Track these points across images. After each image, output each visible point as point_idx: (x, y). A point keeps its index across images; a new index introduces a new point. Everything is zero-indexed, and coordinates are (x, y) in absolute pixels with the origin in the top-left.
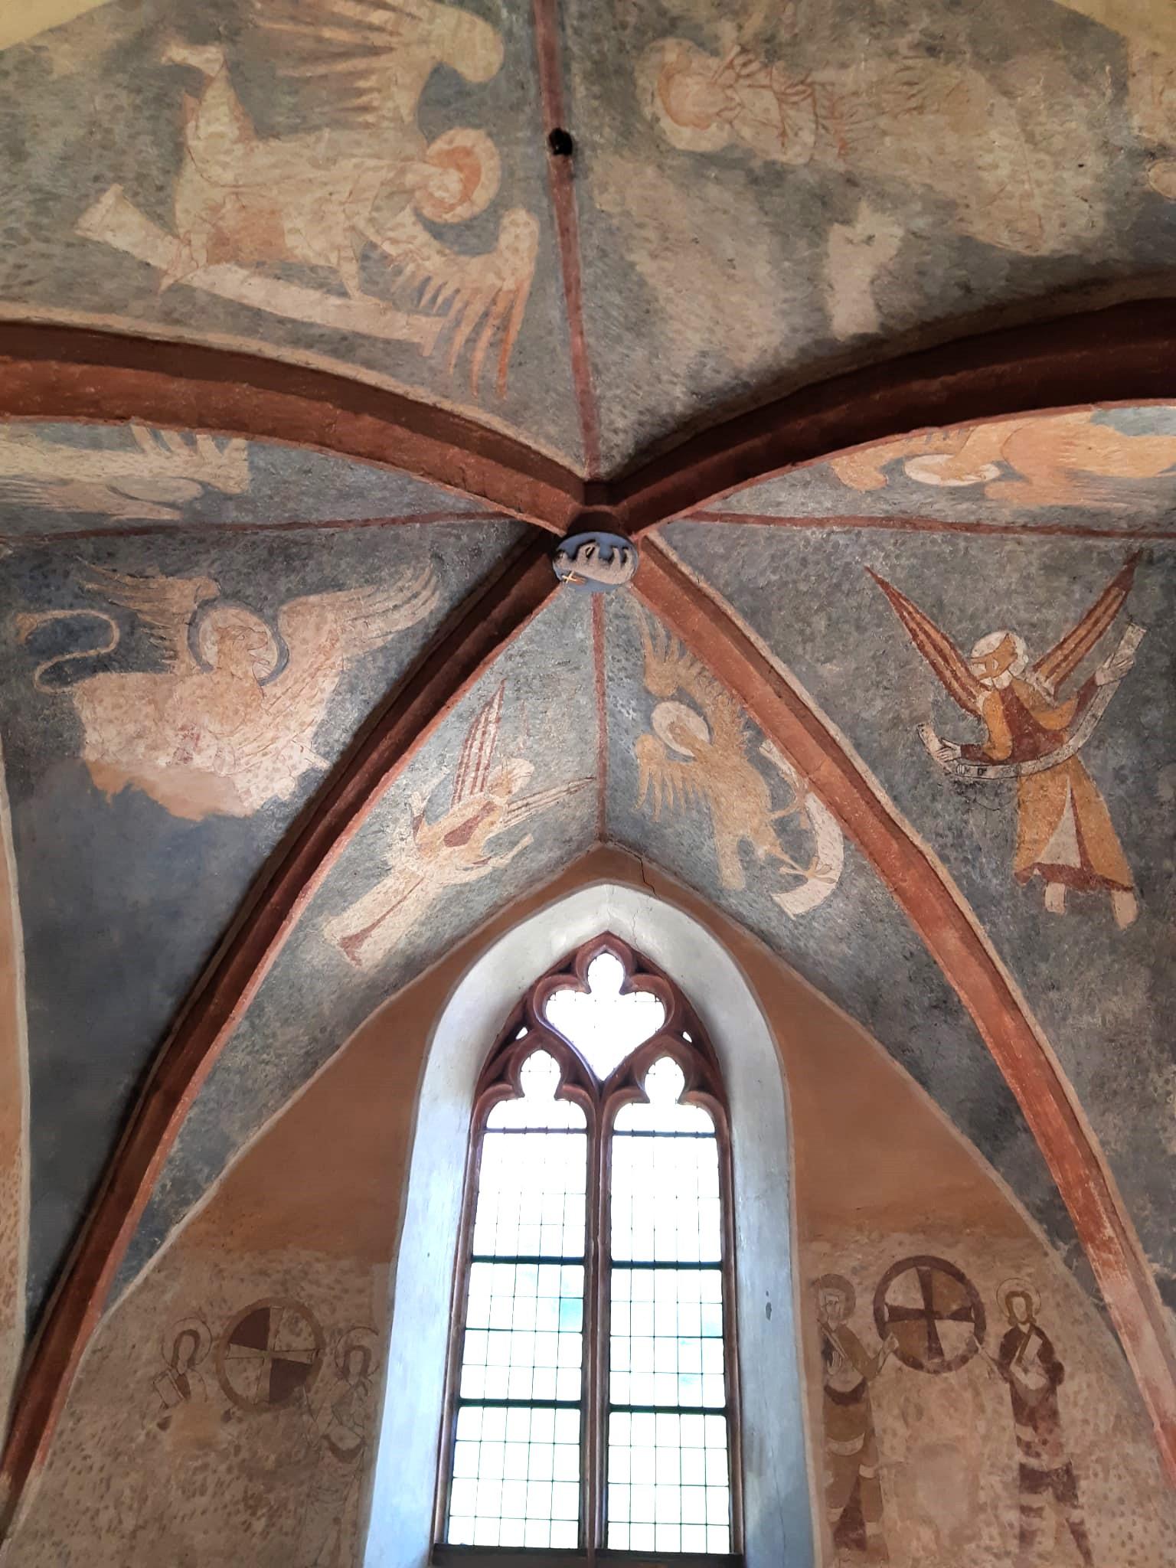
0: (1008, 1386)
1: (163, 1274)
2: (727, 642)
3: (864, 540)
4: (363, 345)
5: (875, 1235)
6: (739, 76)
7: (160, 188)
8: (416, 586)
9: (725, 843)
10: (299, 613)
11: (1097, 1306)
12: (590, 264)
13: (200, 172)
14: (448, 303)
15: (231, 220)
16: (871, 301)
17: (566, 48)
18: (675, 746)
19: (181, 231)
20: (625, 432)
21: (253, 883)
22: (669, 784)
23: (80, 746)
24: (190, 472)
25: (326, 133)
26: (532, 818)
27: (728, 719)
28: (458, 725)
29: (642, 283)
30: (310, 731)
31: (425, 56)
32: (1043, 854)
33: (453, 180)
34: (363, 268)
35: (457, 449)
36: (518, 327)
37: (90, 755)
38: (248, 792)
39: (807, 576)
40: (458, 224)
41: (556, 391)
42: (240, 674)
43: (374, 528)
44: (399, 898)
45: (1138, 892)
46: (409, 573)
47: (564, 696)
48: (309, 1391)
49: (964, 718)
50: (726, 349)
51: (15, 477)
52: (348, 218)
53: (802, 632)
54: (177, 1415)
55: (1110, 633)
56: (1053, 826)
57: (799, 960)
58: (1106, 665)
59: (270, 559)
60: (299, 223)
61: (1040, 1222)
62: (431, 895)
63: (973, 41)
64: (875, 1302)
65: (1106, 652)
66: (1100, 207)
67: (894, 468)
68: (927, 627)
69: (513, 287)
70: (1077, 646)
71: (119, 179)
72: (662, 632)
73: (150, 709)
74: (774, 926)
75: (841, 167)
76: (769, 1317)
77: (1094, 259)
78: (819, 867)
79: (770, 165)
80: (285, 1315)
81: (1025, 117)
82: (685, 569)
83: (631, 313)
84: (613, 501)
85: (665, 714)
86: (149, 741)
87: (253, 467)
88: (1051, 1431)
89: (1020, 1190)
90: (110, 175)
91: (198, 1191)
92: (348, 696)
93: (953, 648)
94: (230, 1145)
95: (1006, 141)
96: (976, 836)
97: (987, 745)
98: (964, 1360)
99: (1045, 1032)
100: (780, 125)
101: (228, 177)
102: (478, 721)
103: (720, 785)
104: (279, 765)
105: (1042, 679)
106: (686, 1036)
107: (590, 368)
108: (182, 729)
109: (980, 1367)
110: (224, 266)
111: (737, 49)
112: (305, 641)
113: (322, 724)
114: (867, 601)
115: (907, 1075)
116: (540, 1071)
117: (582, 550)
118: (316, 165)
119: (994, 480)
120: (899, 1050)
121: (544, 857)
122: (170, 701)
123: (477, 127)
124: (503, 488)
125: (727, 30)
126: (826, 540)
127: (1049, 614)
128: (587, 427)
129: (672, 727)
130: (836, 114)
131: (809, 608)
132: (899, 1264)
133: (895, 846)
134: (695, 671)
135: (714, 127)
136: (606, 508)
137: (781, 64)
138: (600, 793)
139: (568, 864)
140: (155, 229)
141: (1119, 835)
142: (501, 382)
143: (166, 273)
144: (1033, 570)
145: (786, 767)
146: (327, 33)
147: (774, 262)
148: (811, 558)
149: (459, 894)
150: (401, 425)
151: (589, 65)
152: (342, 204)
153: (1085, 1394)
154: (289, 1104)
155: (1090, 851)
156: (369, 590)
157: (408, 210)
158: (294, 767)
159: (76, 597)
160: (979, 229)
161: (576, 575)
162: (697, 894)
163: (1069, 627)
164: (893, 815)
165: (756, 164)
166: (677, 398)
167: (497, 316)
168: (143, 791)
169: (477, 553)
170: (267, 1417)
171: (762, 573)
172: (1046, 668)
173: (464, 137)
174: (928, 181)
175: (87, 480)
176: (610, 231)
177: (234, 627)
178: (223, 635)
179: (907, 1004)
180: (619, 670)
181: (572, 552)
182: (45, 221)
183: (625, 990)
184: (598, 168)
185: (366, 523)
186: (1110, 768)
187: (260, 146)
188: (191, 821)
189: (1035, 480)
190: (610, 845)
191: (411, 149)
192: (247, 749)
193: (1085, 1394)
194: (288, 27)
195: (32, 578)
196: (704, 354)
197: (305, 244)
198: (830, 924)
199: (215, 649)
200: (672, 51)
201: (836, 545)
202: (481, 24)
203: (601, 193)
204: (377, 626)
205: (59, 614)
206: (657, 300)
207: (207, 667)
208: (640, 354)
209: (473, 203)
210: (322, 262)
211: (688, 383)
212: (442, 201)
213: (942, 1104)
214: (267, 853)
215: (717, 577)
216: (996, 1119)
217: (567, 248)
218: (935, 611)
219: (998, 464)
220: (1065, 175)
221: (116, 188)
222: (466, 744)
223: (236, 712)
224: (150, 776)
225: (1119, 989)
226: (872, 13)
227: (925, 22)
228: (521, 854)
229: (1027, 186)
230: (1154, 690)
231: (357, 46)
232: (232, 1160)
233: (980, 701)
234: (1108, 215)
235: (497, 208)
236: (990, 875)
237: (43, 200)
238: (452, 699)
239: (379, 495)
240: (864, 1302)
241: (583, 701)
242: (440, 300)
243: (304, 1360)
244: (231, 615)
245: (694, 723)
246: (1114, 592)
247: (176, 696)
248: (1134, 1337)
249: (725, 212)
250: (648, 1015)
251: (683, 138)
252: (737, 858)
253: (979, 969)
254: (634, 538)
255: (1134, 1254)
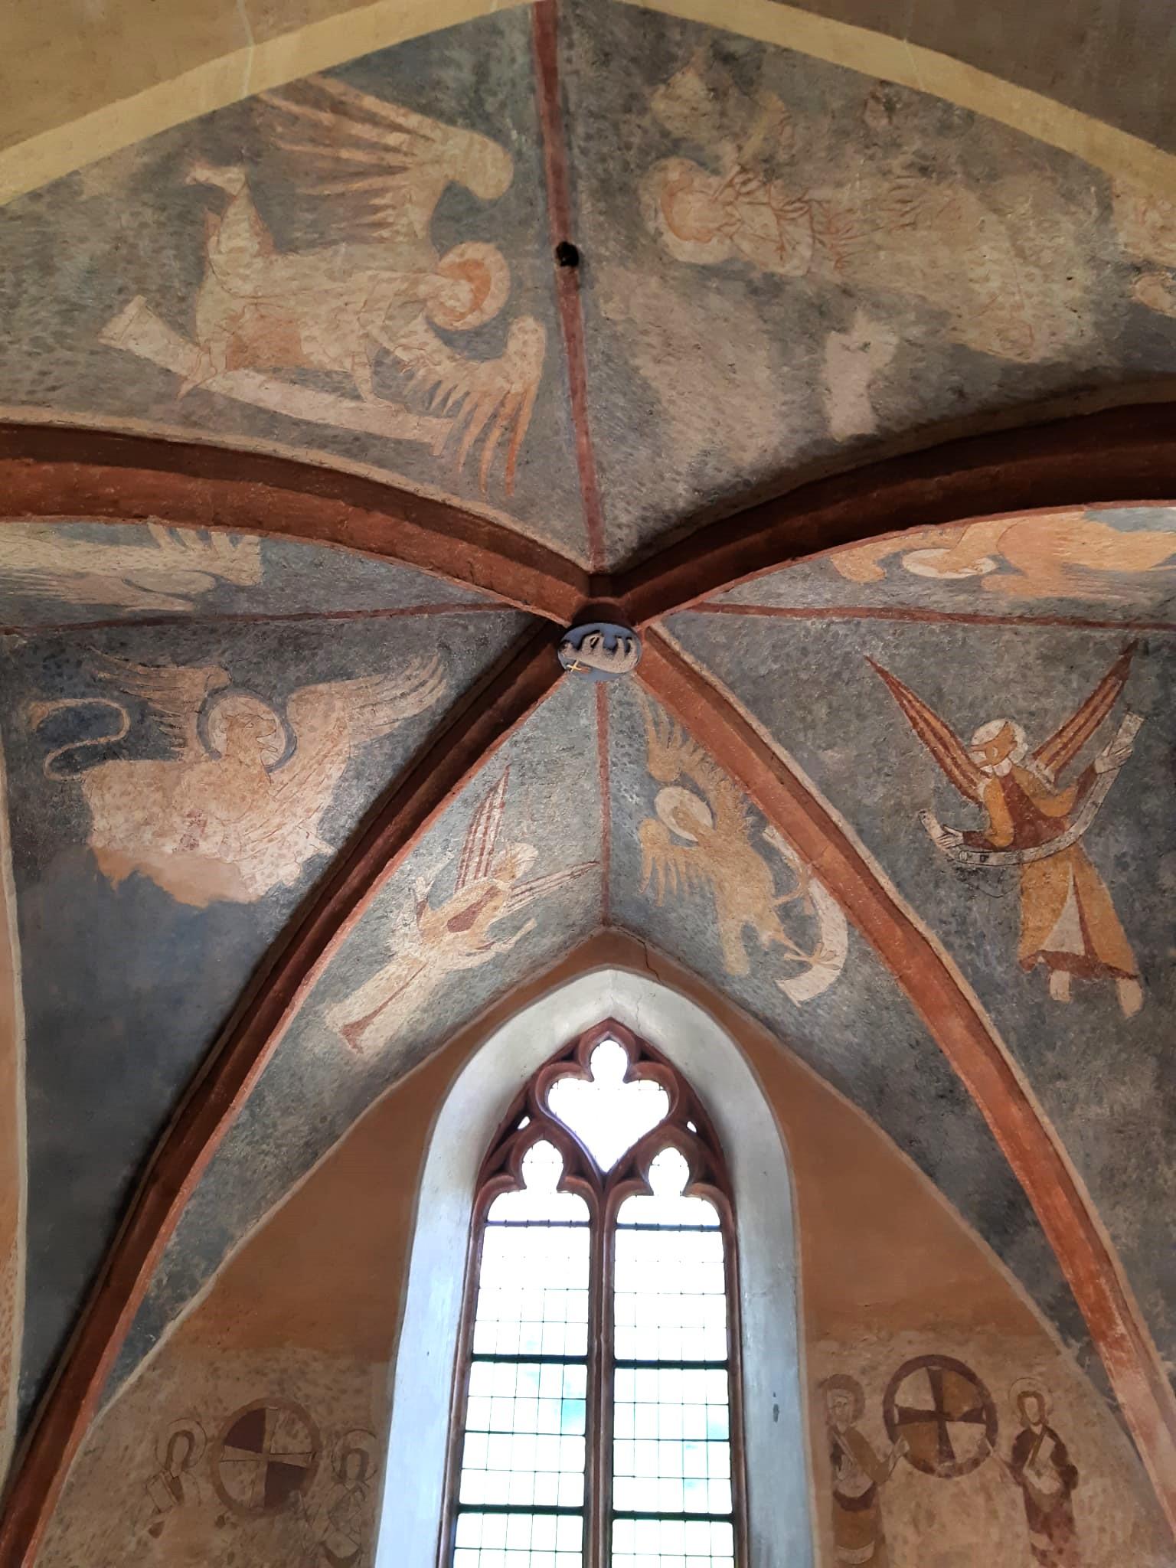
0: (1020, 1490)
1: (158, 1372)
2: (729, 728)
3: (863, 630)
4: (375, 446)
5: (883, 1334)
6: (739, 194)
7: (183, 299)
8: (424, 674)
9: (729, 929)
10: (307, 701)
11: (1110, 1406)
12: (595, 369)
13: (221, 284)
14: (458, 404)
15: (250, 327)
16: (868, 405)
17: (573, 168)
18: (678, 831)
19: (202, 339)
20: (629, 526)
21: (256, 970)
22: (673, 869)
23: (87, 833)
24: (204, 565)
25: (343, 248)
26: (535, 903)
27: (730, 804)
28: (462, 810)
29: (646, 386)
30: (316, 817)
31: (438, 175)
32: (1047, 942)
33: (464, 290)
34: (376, 373)
35: (465, 544)
36: (526, 428)
37: (97, 842)
38: (253, 878)
39: (808, 664)
40: (468, 331)
41: (561, 487)
42: (248, 761)
43: (383, 619)
44: (401, 984)
45: (1142, 979)
46: (417, 662)
47: (569, 781)
48: (305, 1495)
49: (965, 805)
50: (728, 449)
51: (32, 571)
52: (363, 326)
53: (804, 719)
54: (170, 1521)
55: (1108, 721)
56: (1056, 913)
57: (804, 1047)
58: (1105, 754)
59: (281, 649)
60: (316, 331)
61: (1052, 1318)
62: (434, 982)
63: (963, 162)
64: (885, 1402)
65: (1105, 741)
66: (1088, 317)
67: (892, 562)
68: (927, 715)
69: (521, 390)
70: (1075, 734)
71: (143, 291)
72: (664, 718)
73: (158, 796)
74: (778, 1013)
75: (837, 279)
76: (776, 1419)
77: (1084, 366)
78: (824, 953)
79: (769, 277)
80: (282, 1417)
81: (1015, 232)
82: (688, 658)
83: (635, 415)
84: (617, 594)
85: (668, 799)
86: (156, 828)
87: (265, 560)
88: (1066, 1540)
89: (1031, 1285)
90: (134, 287)
91: (195, 1287)
92: (355, 782)
93: (953, 735)
94: (227, 1238)
95: (996, 255)
96: (979, 924)
97: (990, 831)
98: (976, 1463)
99: (1053, 1122)
101: (248, 288)
102: (482, 806)
103: (724, 871)
104: (285, 851)
105: (1042, 766)
106: (691, 1126)
107: (595, 467)
108: (189, 816)
109: (991, 1471)
110: (243, 371)
111: (737, 168)
112: (313, 729)
113: (329, 809)
114: (868, 688)
115: (913, 1166)
116: (542, 1162)
117: (587, 640)
118: (331, 276)
119: (991, 573)
120: (907, 1142)
121: (548, 942)
122: (178, 790)
123: (488, 241)
124: (510, 580)
125: (727, 151)
126: (826, 631)
127: (1047, 702)
128: (592, 522)
129: (675, 812)
130: (833, 230)
131: (810, 696)
132: (909, 1362)
133: (899, 933)
134: (698, 756)
135: (715, 240)
136: (610, 600)
137: (779, 182)
138: (604, 879)
139: (572, 949)
140: (175, 337)
141: (1122, 922)
142: (508, 480)
143: (186, 379)
144: (1030, 659)
145: (789, 853)
146: (345, 154)
148: (811, 648)
149: (462, 980)
150: (412, 521)
151: (595, 183)
152: (358, 313)
153: (1101, 1499)
154: (287, 1196)
155: (1094, 938)
156: (377, 678)
157: (420, 318)
158: (300, 853)
159: (88, 685)
160: (972, 338)
161: (581, 664)
162: (701, 981)
163: (1068, 716)
164: (896, 902)
165: (756, 276)
166: (680, 495)
167: (505, 416)
168: (149, 878)
169: (484, 642)
170: (262, 1522)
171: (763, 662)
172: (1046, 755)
173: (474, 251)
174: (921, 292)
175: (102, 573)
176: (615, 337)
177: (243, 715)
178: (232, 722)
179: (913, 1093)
180: (624, 755)
181: (577, 642)
182: (70, 330)
183: (629, 1078)
184: (602, 277)
185: (376, 613)
186: (1112, 855)
187: (279, 261)
188: (195, 908)
189: (1030, 572)
190: (614, 929)
191: (423, 262)
192: (253, 835)
193: (1101, 1499)
194: (308, 148)
195: (45, 667)
196: (706, 453)
197: (321, 349)
198: (834, 1012)
199: (224, 736)
200: (674, 170)
201: (836, 635)
202: (492, 145)
203: (606, 302)
204: (384, 714)
205: (70, 702)
206: (659, 402)
207: (215, 754)
208: (644, 453)
209: (482, 311)
210: (337, 368)
211: (689, 479)
212: (453, 310)
213: (950, 1196)
214: (271, 940)
215: (719, 665)
216: (1005, 1213)
217: (574, 353)
218: (934, 699)
219: (994, 558)
220: (1055, 287)
221: (140, 299)
222: (471, 829)
223: (243, 798)
224: (155, 861)
225: (1127, 1079)
226: (867, 136)
227: (917, 144)
228: (524, 939)
229: (1017, 298)
230: (1153, 778)
231: (373, 166)
232: (230, 1254)
233: (982, 788)
234: (1097, 325)
235: (506, 316)
236: (994, 962)
237: (69, 311)
238: (457, 785)
239: (389, 587)
240: (874, 1403)
241: (587, 786)
242: (450, 402)
243: (300, 1462)
244: (239, 704)
245: (698, 809)
246: (1111, 682)
247: (184, 783)
248: (1149, 1438)
249: (726, 320)
250: (651, 1104)
251: (685, 251)
252: (741, 944)
253: (984, 1058)
254: (637, 628)
255: (1147, 1352)
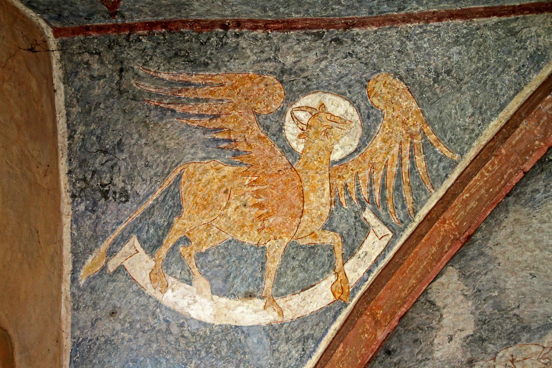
16: (439, 304)
100: (515, 364)
147: (502, 291)
165: (525, 336)
